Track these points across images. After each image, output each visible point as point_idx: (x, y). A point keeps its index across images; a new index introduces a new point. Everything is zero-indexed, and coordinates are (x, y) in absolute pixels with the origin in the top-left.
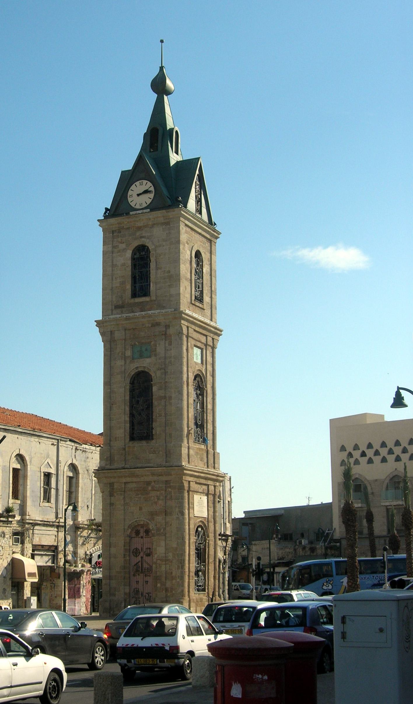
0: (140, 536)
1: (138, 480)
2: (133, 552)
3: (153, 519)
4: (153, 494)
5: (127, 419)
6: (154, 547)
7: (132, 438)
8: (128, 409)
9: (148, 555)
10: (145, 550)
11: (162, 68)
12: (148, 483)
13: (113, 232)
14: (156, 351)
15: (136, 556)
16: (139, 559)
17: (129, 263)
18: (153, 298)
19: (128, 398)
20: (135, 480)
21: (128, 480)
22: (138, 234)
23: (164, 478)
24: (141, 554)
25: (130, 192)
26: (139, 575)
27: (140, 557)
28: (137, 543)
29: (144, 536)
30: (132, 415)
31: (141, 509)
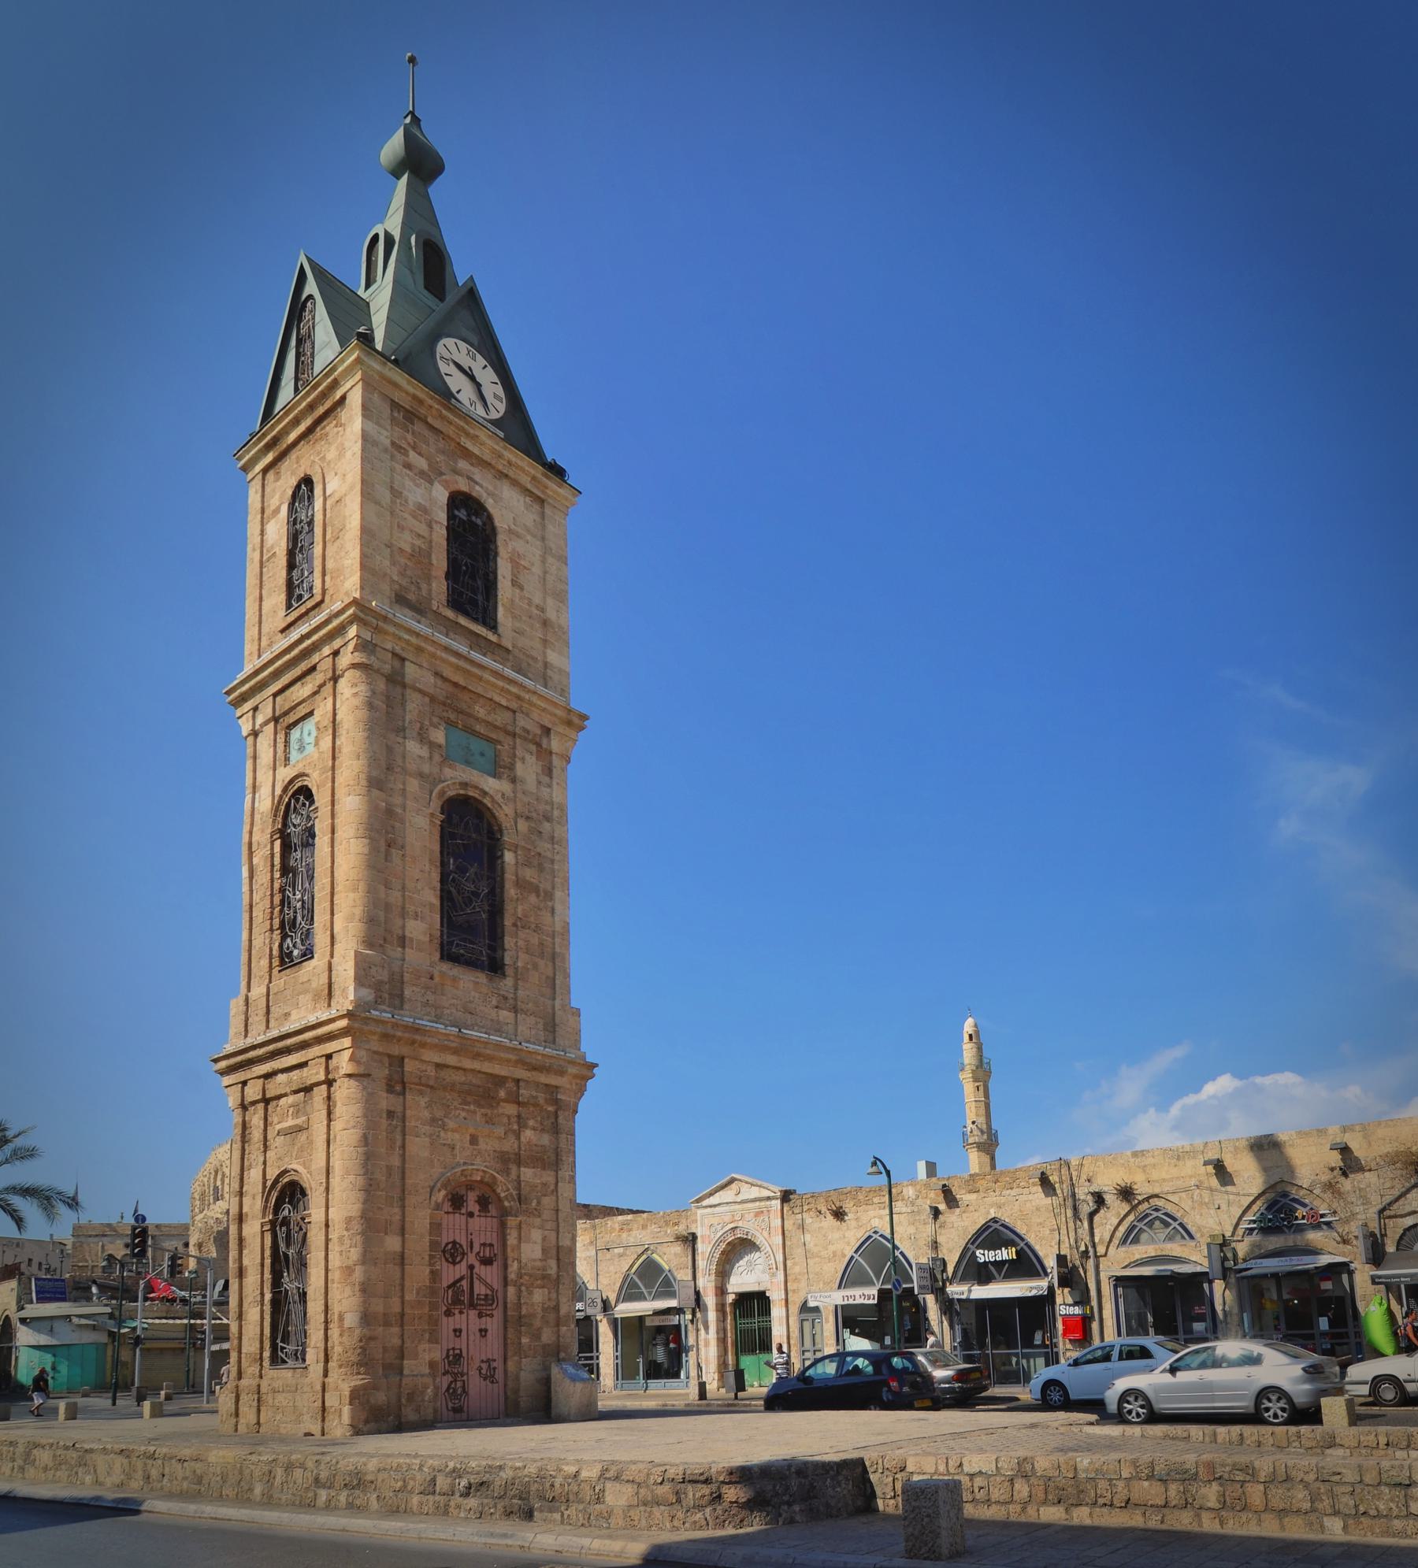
0: (463, 1211)
1: (476, 1065)
2: (444, 1251)
5: (437, 902)
7: (448, 955)
8: (436, 876)
10: (476, 1248)
11: (416, 120)
15: (454, 1263)
16: (461, 1269)
19: (437, 848)
20: (468, 1064)
21: (451, 1060)
22: (462, 464)
24: (472, 1259)
26: (461, 1313)
28: (455, 1228)
29: (477, 1213)
30: (446, 897)
31: (474, 1140)
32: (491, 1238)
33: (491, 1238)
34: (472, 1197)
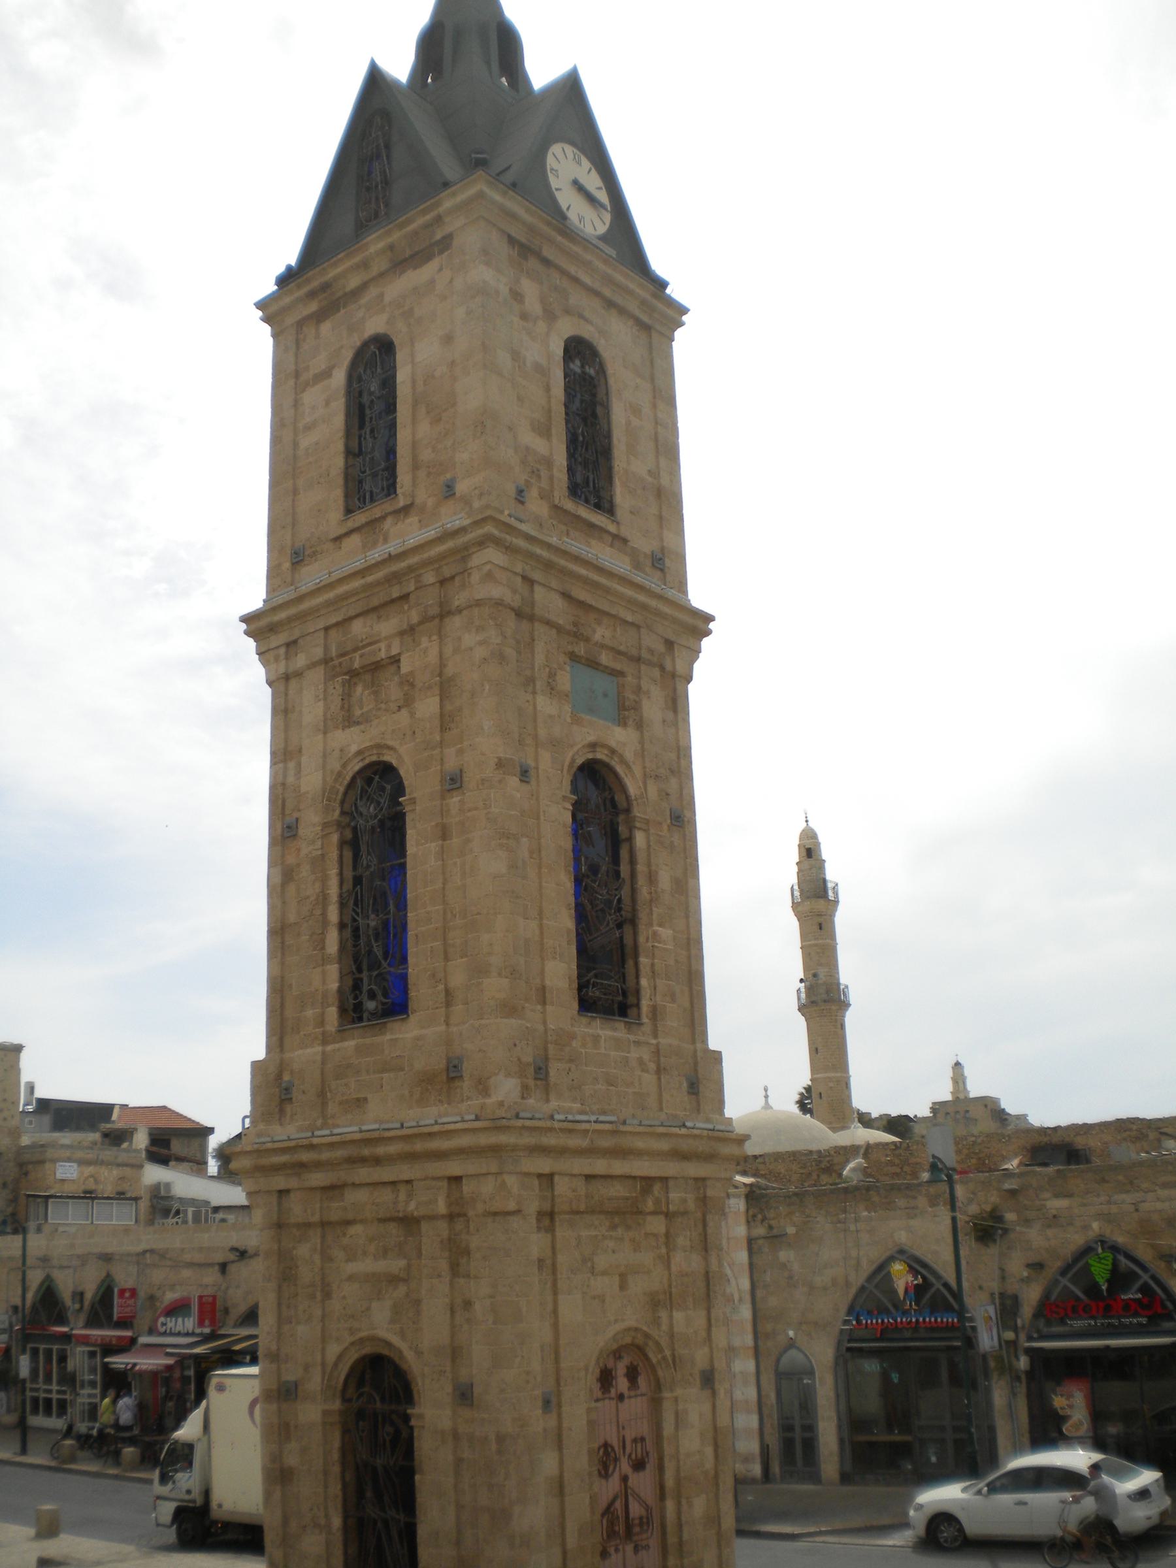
3: (656, 1322)
4: (657, 1225)
6: (668, 1428)
9: (639, 1465)
12: (648, 1182)
13: (512, 240)
14: (637, 707)
17: (558, 375)
18: (625, 532)
20: (619, 1167)
23: (693, 1169)
25: (550, 161)
26: (617, 1550)
27: (616, 1476)
29: (626, 1393)
30: (581, 916)
32: (644, 1429)
33: (644, 1429)
34: (621, 1370)
